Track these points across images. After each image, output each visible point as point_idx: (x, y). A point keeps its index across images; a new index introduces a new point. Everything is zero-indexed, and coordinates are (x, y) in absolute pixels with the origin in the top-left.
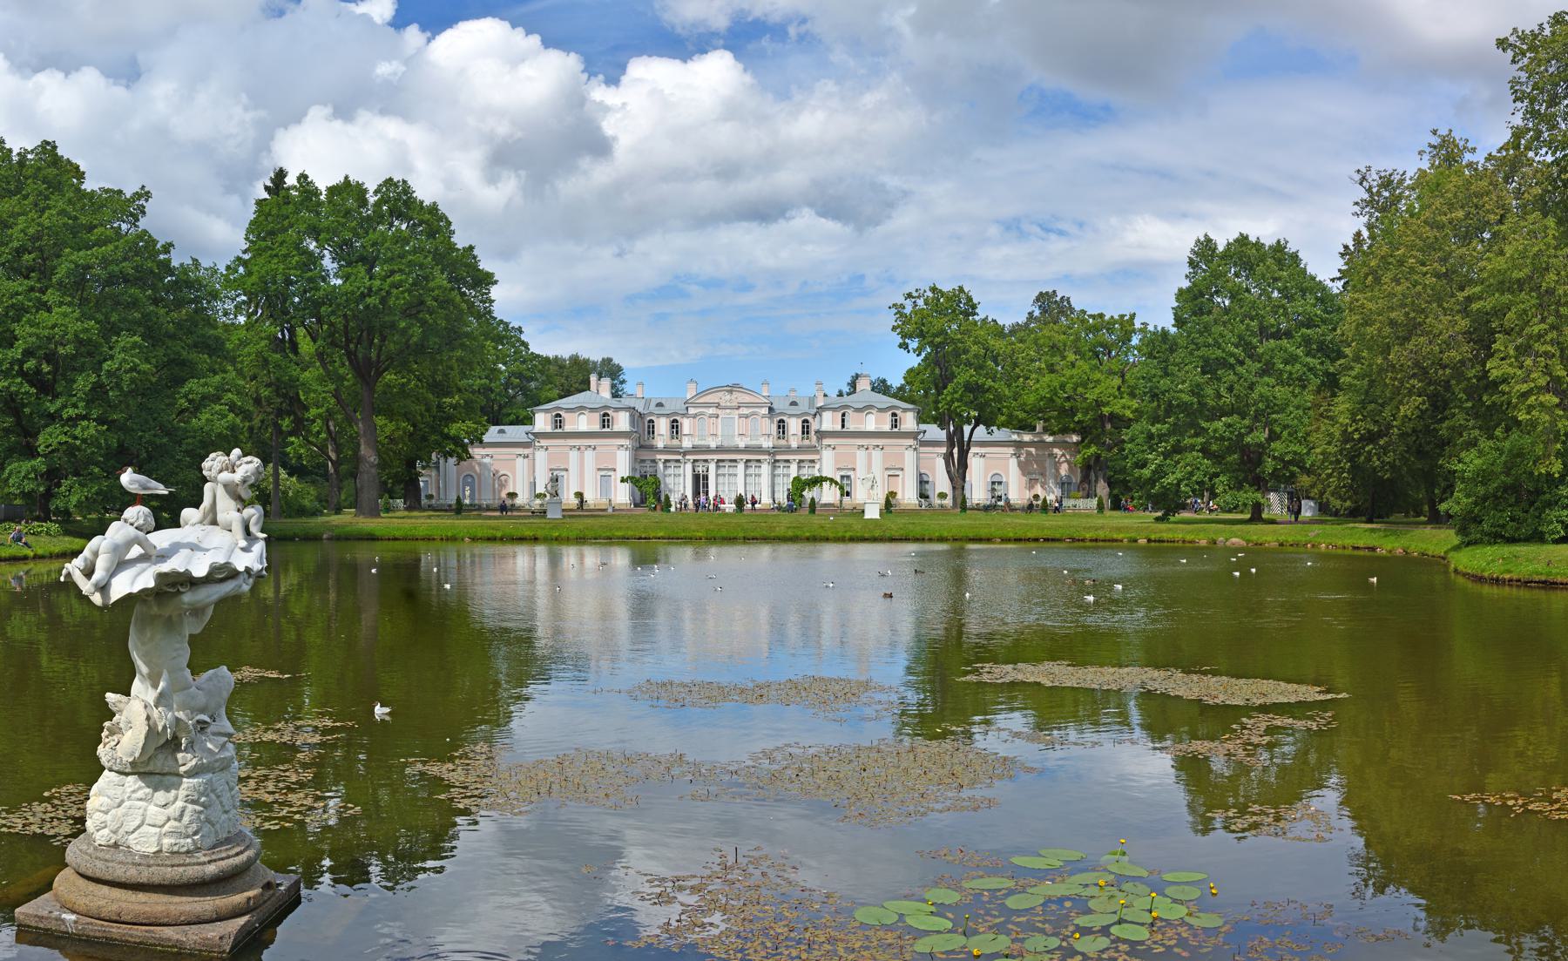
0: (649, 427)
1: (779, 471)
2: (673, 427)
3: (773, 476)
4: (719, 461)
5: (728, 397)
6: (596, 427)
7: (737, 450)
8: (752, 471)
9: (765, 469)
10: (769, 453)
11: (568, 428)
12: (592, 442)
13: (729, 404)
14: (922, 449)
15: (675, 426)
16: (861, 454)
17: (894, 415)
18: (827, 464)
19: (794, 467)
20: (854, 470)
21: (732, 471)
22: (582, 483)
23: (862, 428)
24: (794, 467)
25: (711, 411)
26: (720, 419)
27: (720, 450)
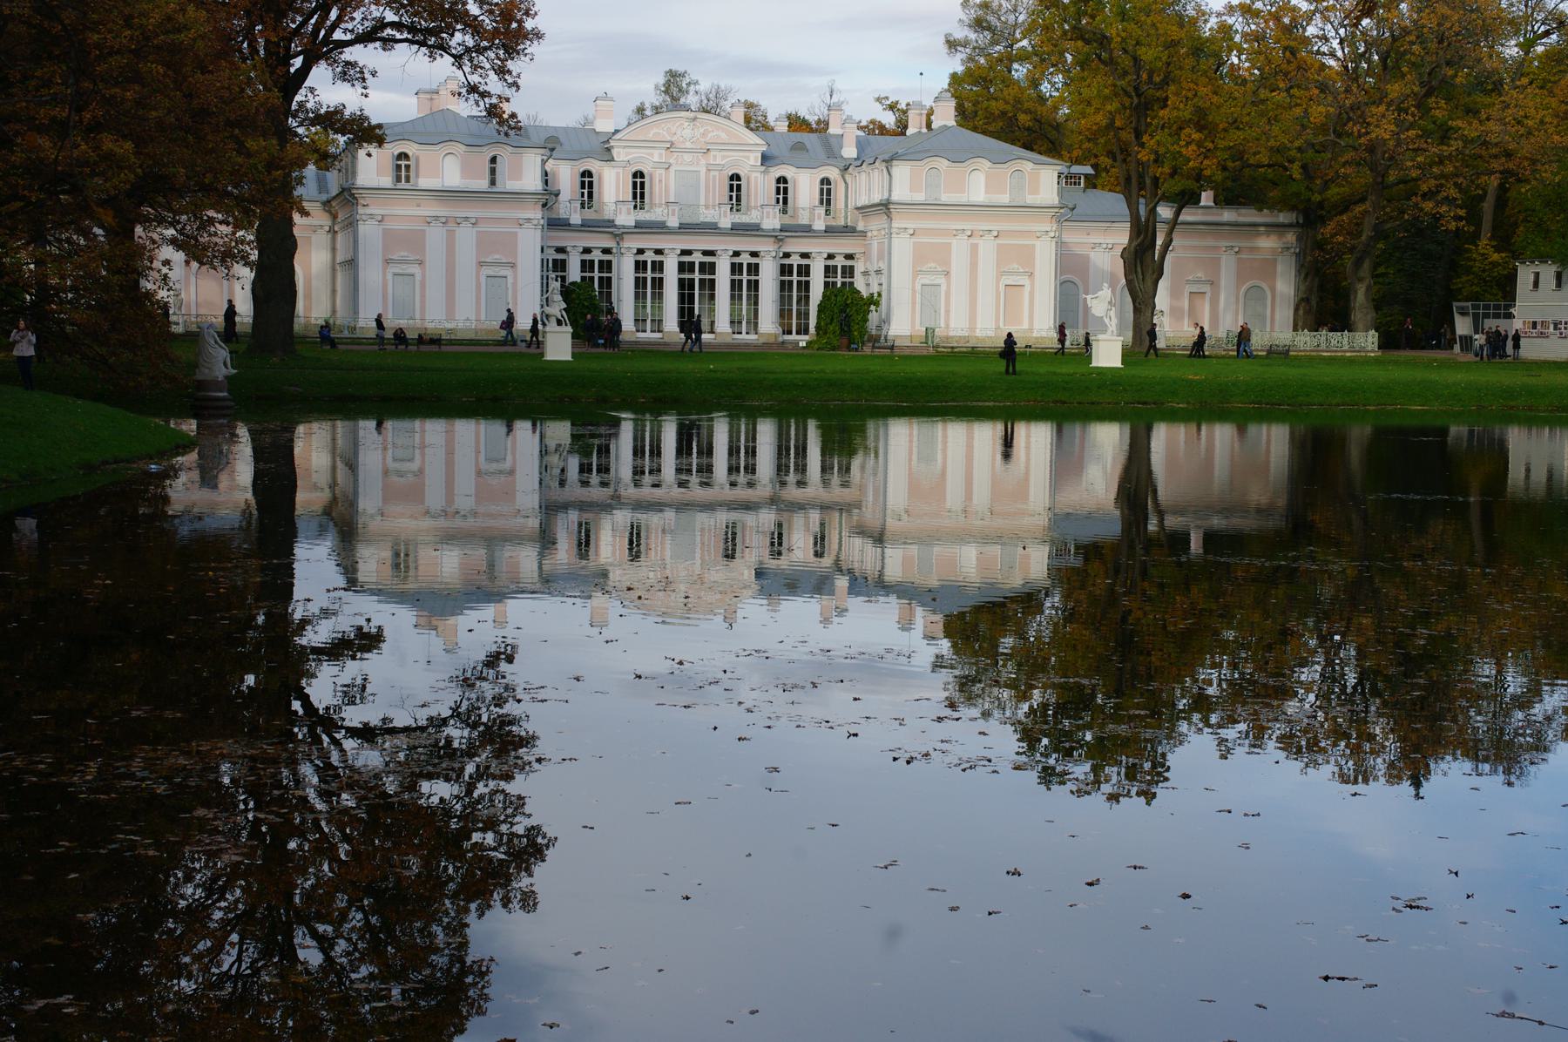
2: (583, 185)
5: (687, 132)
7: (711, 229)
11: (424, 182)
12: (473, 213)
13: (688, 145)
15: (587, 181)
20: (947, 274)
23: (963, 199)
26: (672, 169)
27: (686, 228)
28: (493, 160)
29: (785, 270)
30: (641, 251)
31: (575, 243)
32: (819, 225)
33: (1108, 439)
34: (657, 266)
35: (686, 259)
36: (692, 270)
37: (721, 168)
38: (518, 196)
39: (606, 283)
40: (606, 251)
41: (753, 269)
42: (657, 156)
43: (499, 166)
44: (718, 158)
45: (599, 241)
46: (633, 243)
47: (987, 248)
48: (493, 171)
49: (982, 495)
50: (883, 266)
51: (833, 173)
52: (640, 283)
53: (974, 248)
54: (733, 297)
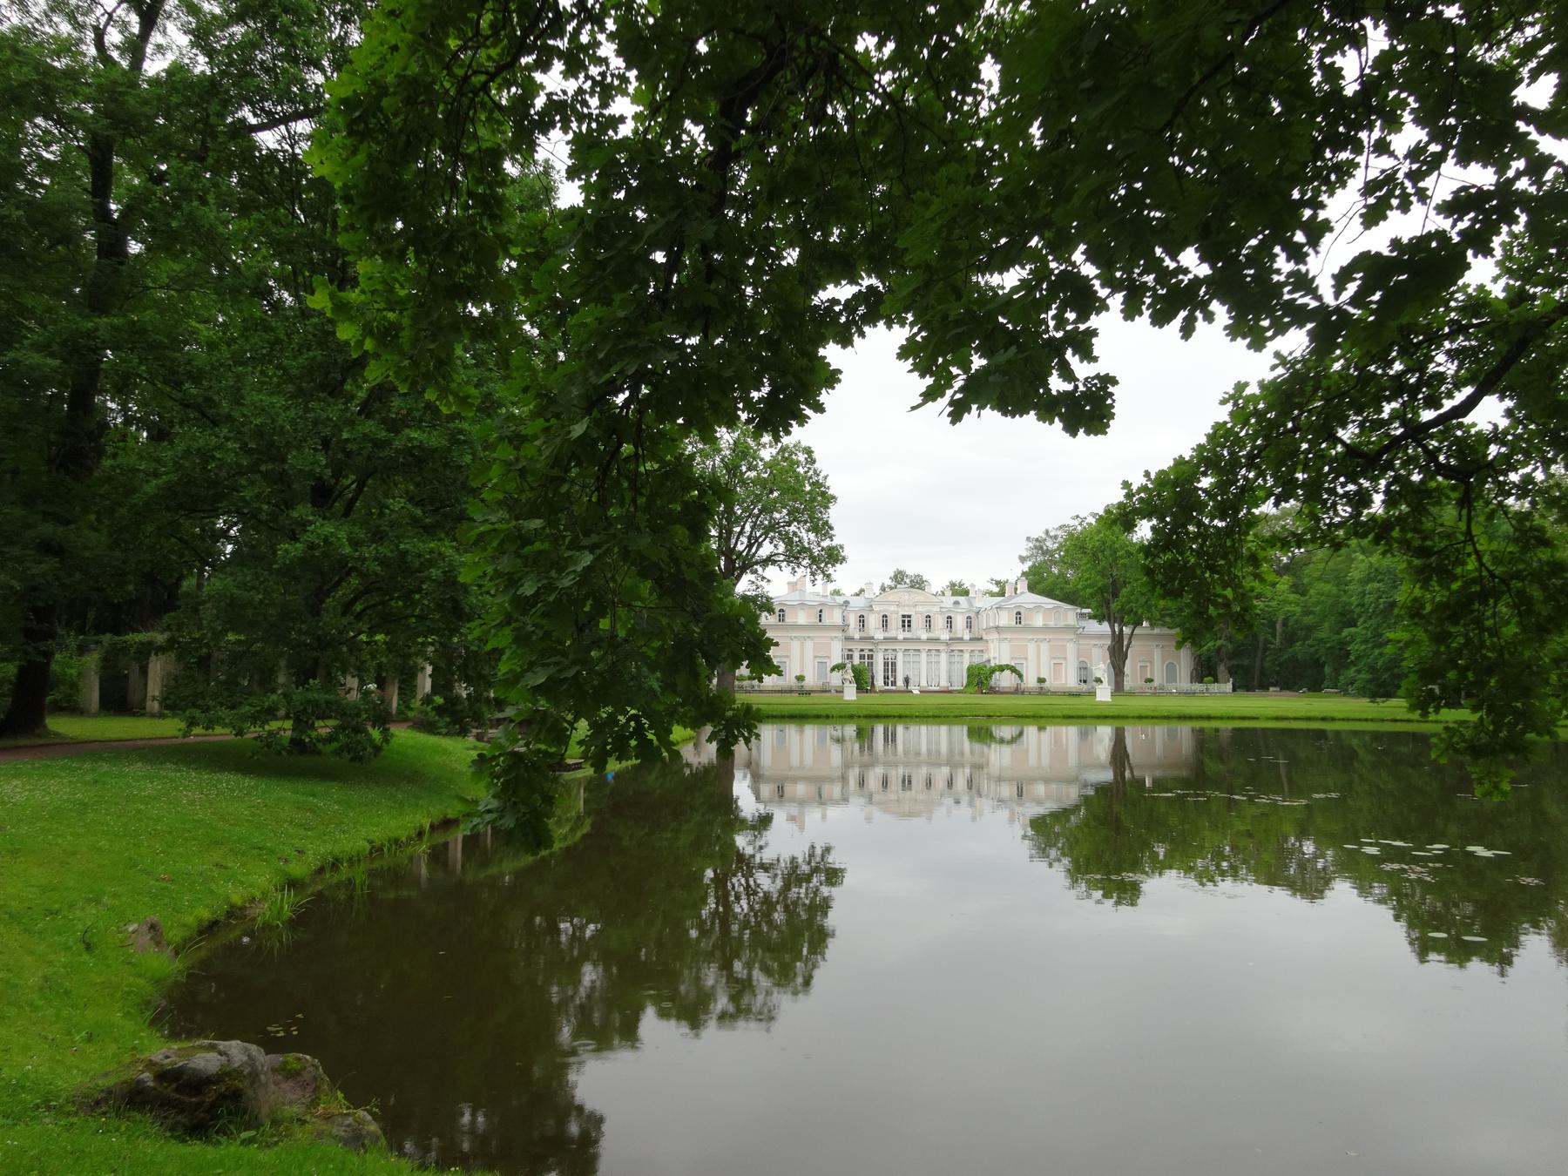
1: (956, 659)
3: (950, 663)
6: (815, 620)
8: (933, 659)
9: (944, 657)
14: (1081, 642)
15: (862, 620)
16: (1031, 647)
17: (1019, 613)
18: (998, 652)
19: (966, 656)
21: (916, 659)
22: (802, 668)
24: (966, 656)
31: (856, 647)
32: (967, 637)
33: (1105, 733)
37: (921, 613)
38: (833, 627)
39: (871, 664)
42: (893, 608)
44: (920, 609)
45: (867, 646)
46: (883, 647)
47: (1044, 647)
49: (1046, 761)
50: (997, 655)
51: (972, 615)
53: (1039, 646)
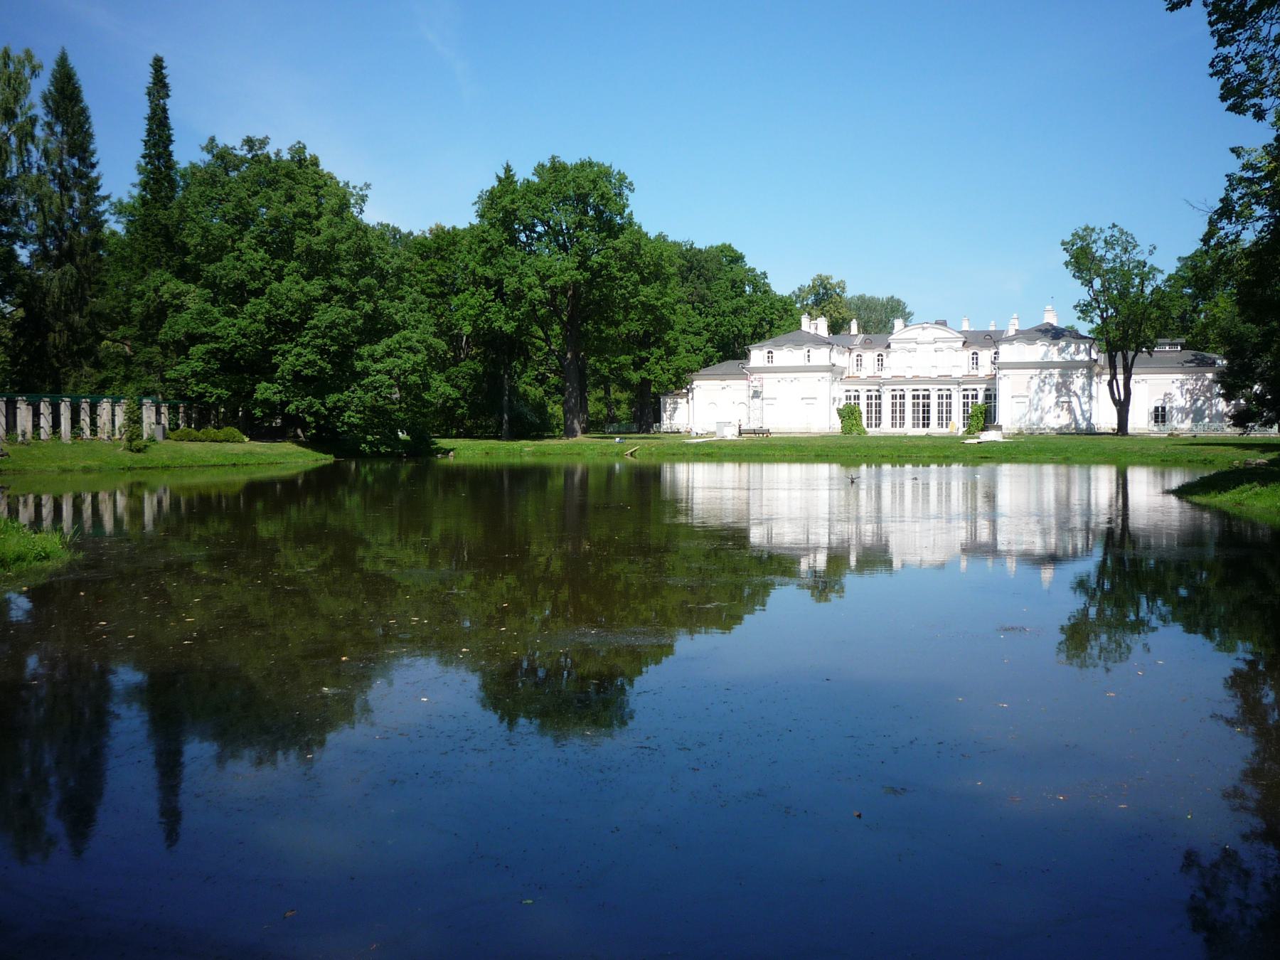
0: (857, 360)
4: (914, 390)
10: (959, 384)
25: (913, 345)
28: (809, 351)
29: (966, 397)
30: (894, 390)
34: (902, 397)
35: (916, 393)
36: (918, 398)
40: (878, 391)
41: (949, 397)
43: (810, 354)
48: (809, 356)
52: (894, 405)
54: (928, 412)
